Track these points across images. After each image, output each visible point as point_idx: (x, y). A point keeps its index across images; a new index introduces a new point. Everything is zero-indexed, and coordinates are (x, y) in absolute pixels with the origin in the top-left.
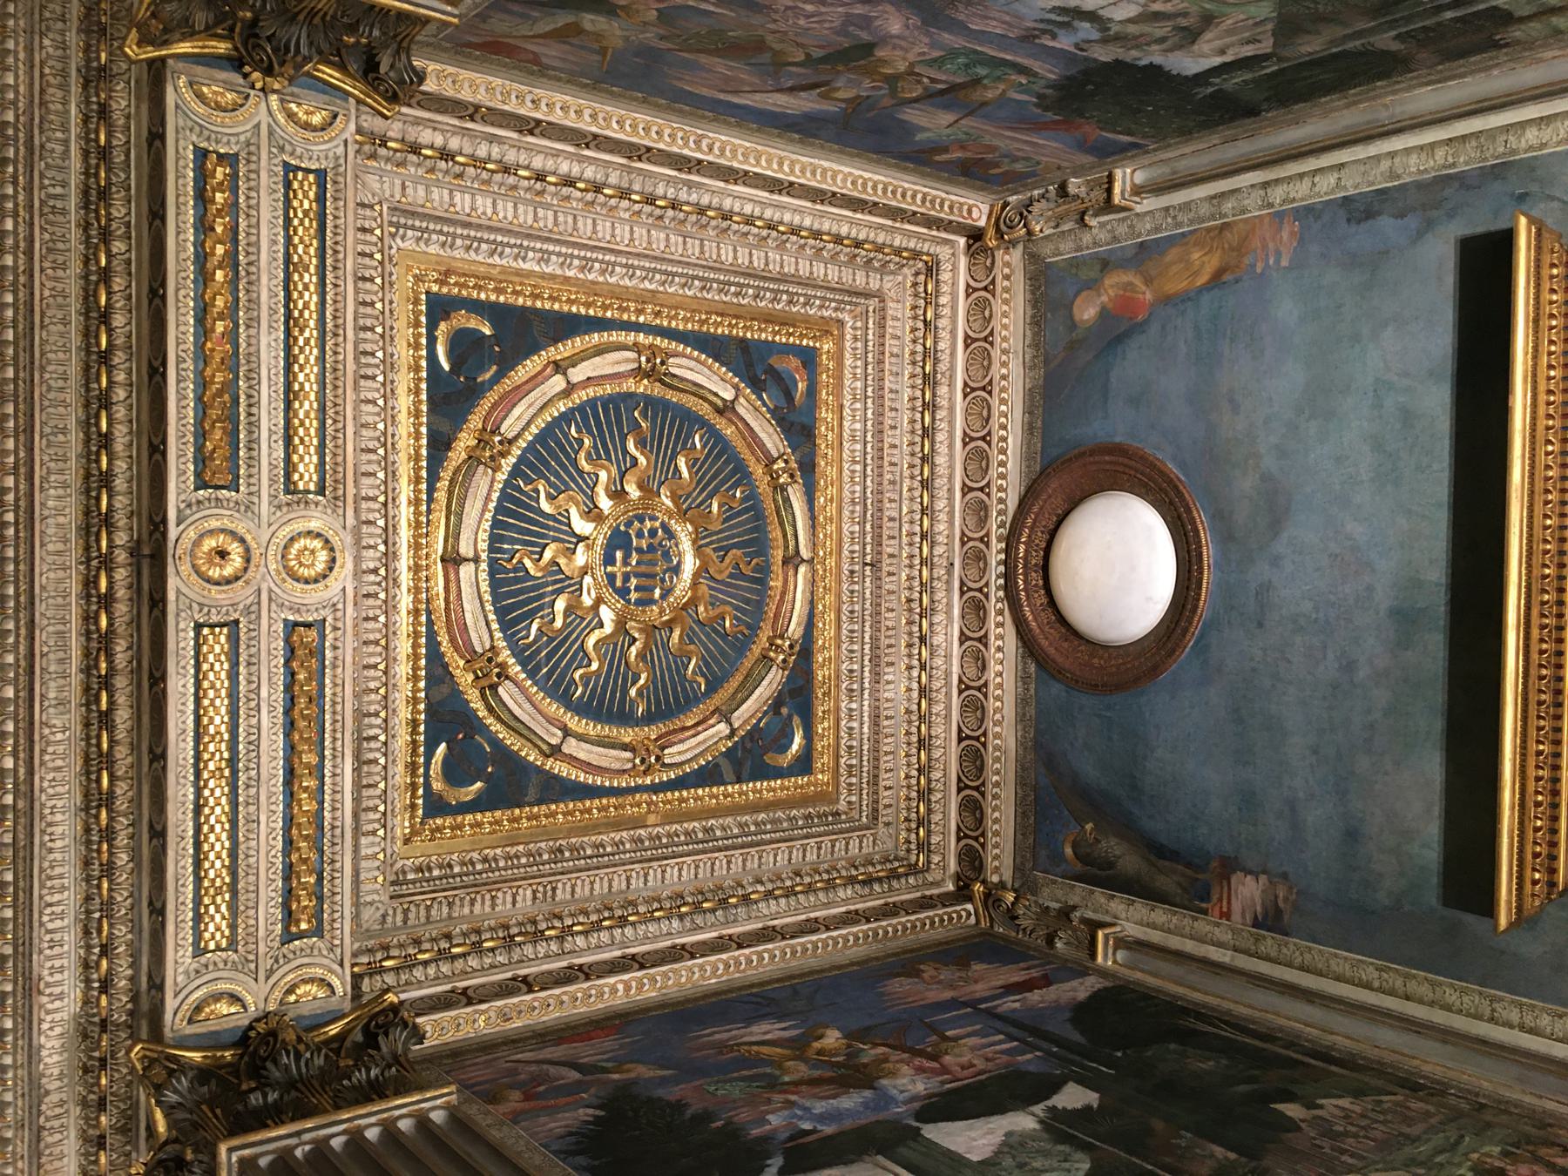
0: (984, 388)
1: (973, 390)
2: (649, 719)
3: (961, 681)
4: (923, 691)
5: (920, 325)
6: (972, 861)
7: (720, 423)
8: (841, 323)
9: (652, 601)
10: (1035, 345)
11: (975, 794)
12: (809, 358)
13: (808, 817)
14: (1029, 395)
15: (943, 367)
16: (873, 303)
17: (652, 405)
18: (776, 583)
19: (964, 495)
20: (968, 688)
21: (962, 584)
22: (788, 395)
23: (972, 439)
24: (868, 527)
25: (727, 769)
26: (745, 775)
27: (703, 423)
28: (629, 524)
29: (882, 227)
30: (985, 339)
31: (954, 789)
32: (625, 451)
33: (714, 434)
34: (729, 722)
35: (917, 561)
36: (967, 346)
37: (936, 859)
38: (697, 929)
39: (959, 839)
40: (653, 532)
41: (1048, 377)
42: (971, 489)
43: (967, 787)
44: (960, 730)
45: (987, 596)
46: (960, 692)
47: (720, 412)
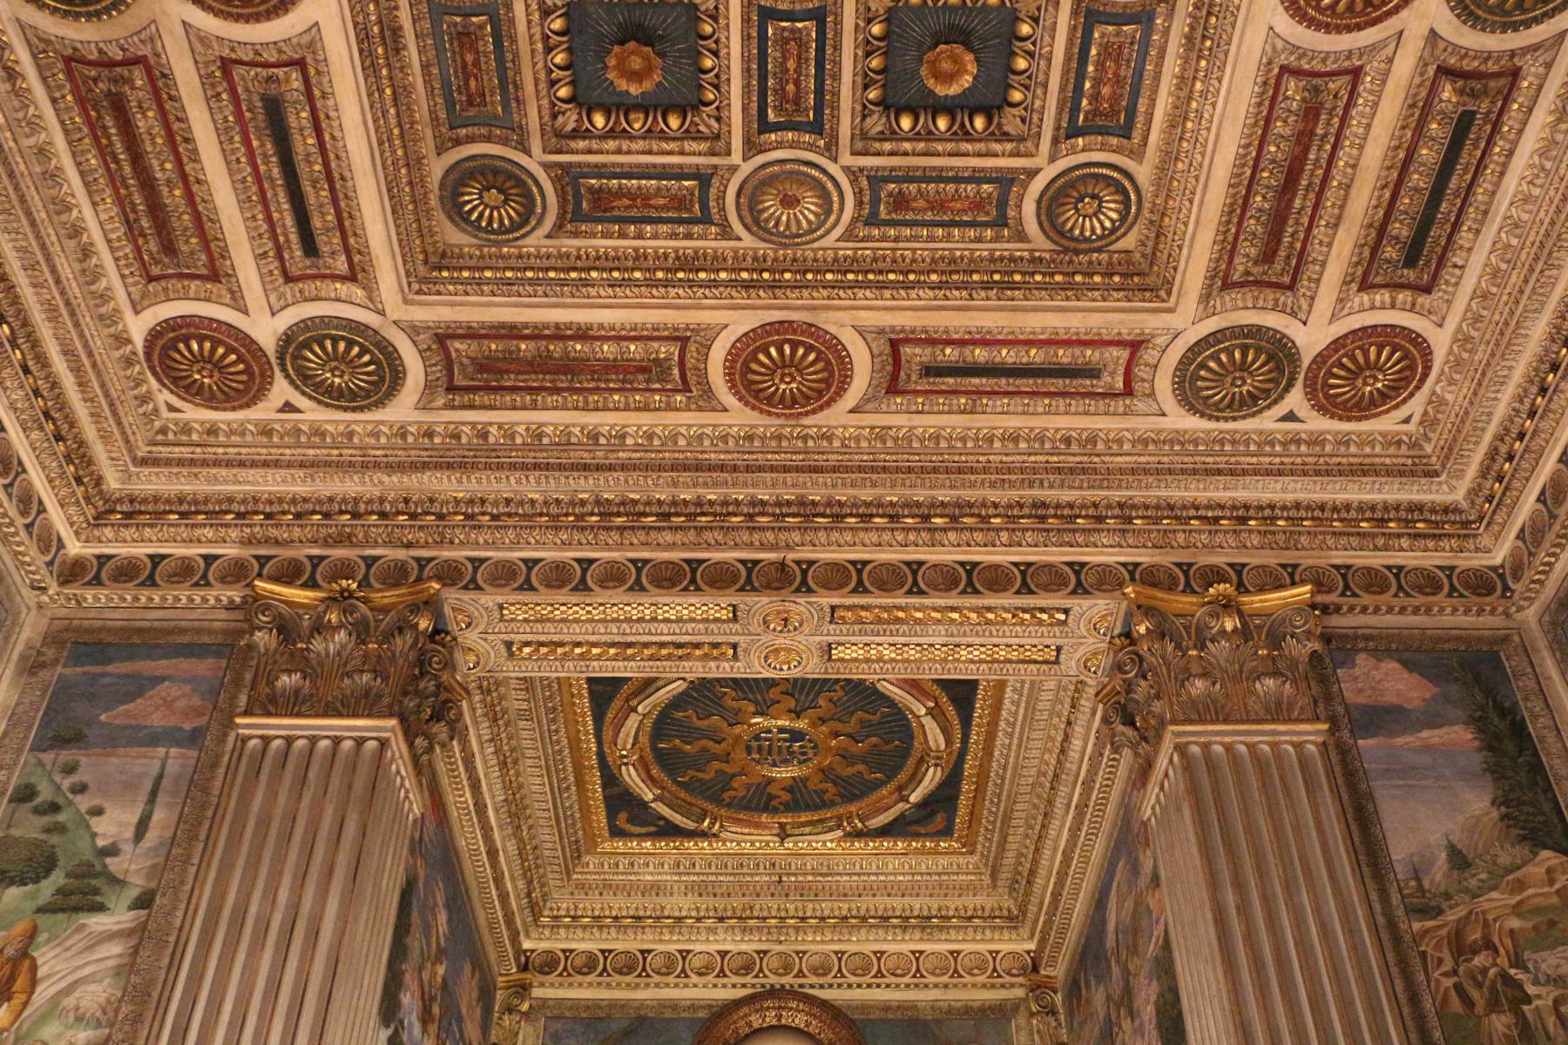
0: (918, 970)
1: (917, 959)
2: (654, 748)
3: (688, 952)
4: (680, 919)
5: (970, 913)
6: (548, 964)
7: (891, 786)
8: (971, 853)
9: (749, 753)
10: (950, 1011)
11: (601, 967)
12: (947, 832)
13: (577, 841)
14: (912, 1006)
15: (937, 935)
16: (987, 879)
17: (905, 753)
18: (764, 818)
19: (836, 953)
20: (684, 959)
21: (765, 952)
22: (917, 822)
23: (879, 959)
24: (810, 878)
25: (615, 791)
26: (594, 687)
27: (890, 778)
28: (810, 741)
29: (1042, 903)
30: (956, 971)
31: (604, 947)
32: (867, 737)
33: (880, 784)
34: (654, 800)
35: (783, 914)
36: (952, 953)
37: (547, 932)
38: (497, 811)
39: (564, 951)
40: (804, 754)
41: (925, 1022)
42: (840, 960)
43: (606, 958)
44: (649, 951)
45: (756, 976)
46: (680, 952)
47: (900, 789)
